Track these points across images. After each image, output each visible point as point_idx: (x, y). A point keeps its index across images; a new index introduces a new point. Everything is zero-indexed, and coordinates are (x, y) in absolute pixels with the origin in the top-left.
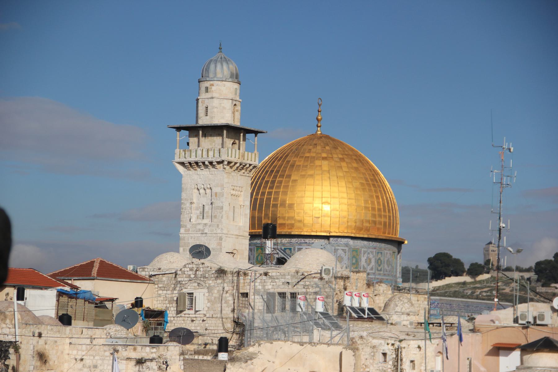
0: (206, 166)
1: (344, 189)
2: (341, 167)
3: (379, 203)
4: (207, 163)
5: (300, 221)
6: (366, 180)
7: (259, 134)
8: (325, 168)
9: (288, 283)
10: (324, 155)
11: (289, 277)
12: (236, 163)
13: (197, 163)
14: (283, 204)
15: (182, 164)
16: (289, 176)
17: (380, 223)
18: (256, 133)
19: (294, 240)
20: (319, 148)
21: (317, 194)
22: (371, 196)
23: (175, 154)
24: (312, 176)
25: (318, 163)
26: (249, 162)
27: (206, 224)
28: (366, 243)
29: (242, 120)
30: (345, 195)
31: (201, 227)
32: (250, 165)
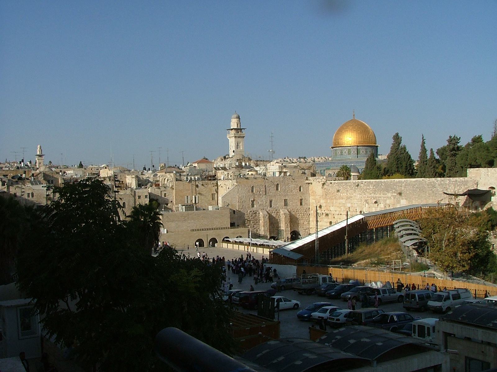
1: (355, 134)
2: (355, 128)
3: (366, 137)
5: (344, 143)
6: (362, 130)
7: (245, 129)
8: (351, 128)
10: (351, 125)
12: (237, 136)
14: (340, 139)
16: (342, 131)
17: (366, 141)
18: (244, 129)
19: (343, 147)
20: (351, 123)
21: (348, 135)
22: (363, 135)
24: (347, 131)
25: (349, 127)
26: (242, 135)
28: (361, 147)
29: (240, 127)
30: (355, 135)
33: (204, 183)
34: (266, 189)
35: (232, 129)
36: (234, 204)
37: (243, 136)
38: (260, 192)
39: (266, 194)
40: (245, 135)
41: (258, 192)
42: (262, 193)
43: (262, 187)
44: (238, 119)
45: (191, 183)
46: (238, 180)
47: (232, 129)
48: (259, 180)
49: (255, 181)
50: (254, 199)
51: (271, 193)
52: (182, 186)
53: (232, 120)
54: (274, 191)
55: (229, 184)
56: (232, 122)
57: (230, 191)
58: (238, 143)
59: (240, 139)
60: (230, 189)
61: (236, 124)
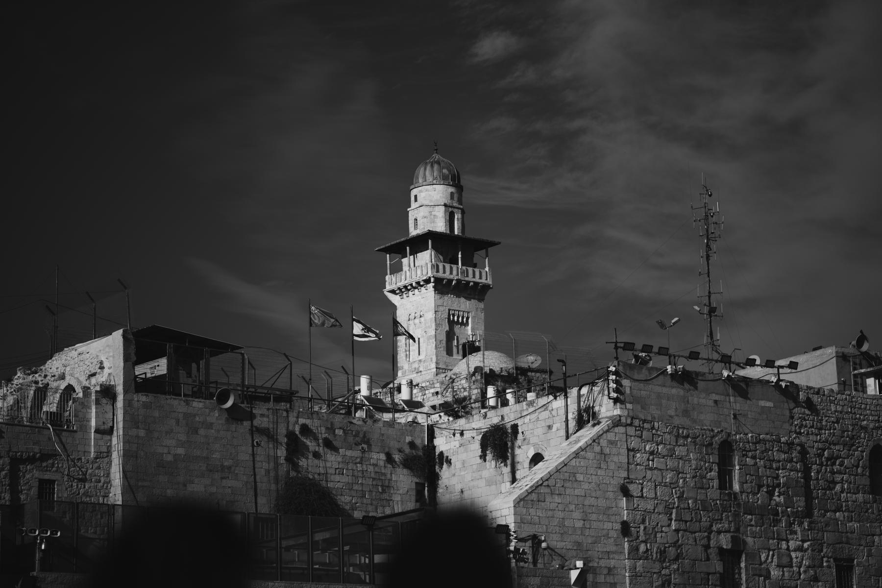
0: (415, 288)
4: (414, 285)
9: (437, 393)
11: (438, 385)
12: (451, 281)
13: (405, 287)
15: (393, 292)
23: (385, 281)
26: (477, 279)
27: (420, 361)
31: (416, 365)
32: (476, 284)
33: (339, 432)
34: (806, 471)
35: (418, 244)
36: (603, 563)
37: (483, 281)
38: (771, 494)
39: (808, 513)
40: (489, 281)
41: (760, 487)
42: (789, 503)
43: (783, 456)
44: (451, 189)
45: (247, 424)
46: (626, 383)
47: (418, 244)
48: (762, 403)
49: (737, 404)
50: (735, 540)
51: (839, 509)
52: (183, 437)
53: (414, 192)
54: (860, 496)
55: (539, 431)
56: (414, 205)
57: (577, 454)
58: (452, 323)
59: (463, 305)
60: (542, 470)
61: (440, 212)
